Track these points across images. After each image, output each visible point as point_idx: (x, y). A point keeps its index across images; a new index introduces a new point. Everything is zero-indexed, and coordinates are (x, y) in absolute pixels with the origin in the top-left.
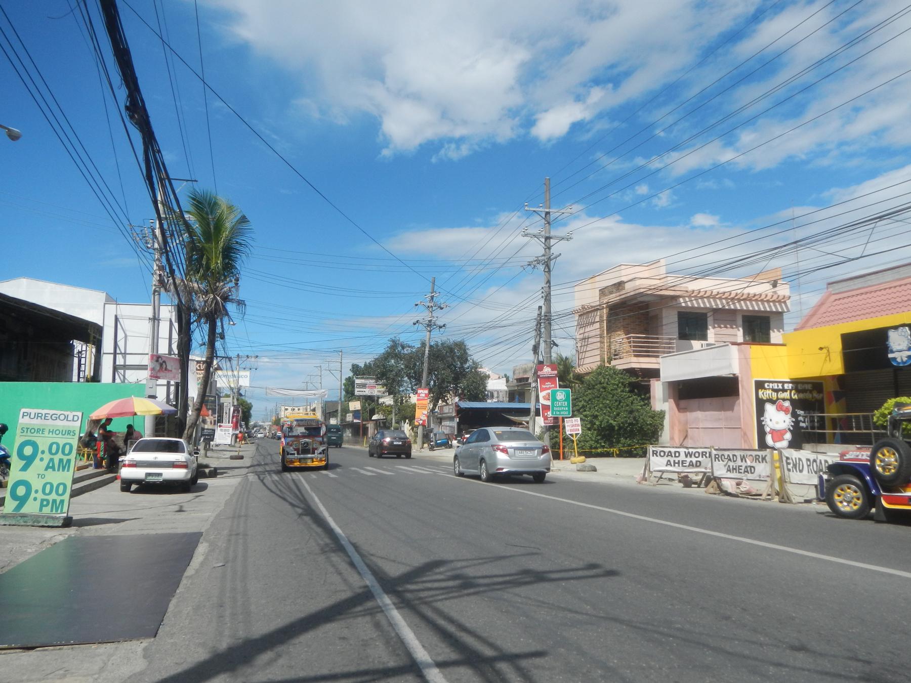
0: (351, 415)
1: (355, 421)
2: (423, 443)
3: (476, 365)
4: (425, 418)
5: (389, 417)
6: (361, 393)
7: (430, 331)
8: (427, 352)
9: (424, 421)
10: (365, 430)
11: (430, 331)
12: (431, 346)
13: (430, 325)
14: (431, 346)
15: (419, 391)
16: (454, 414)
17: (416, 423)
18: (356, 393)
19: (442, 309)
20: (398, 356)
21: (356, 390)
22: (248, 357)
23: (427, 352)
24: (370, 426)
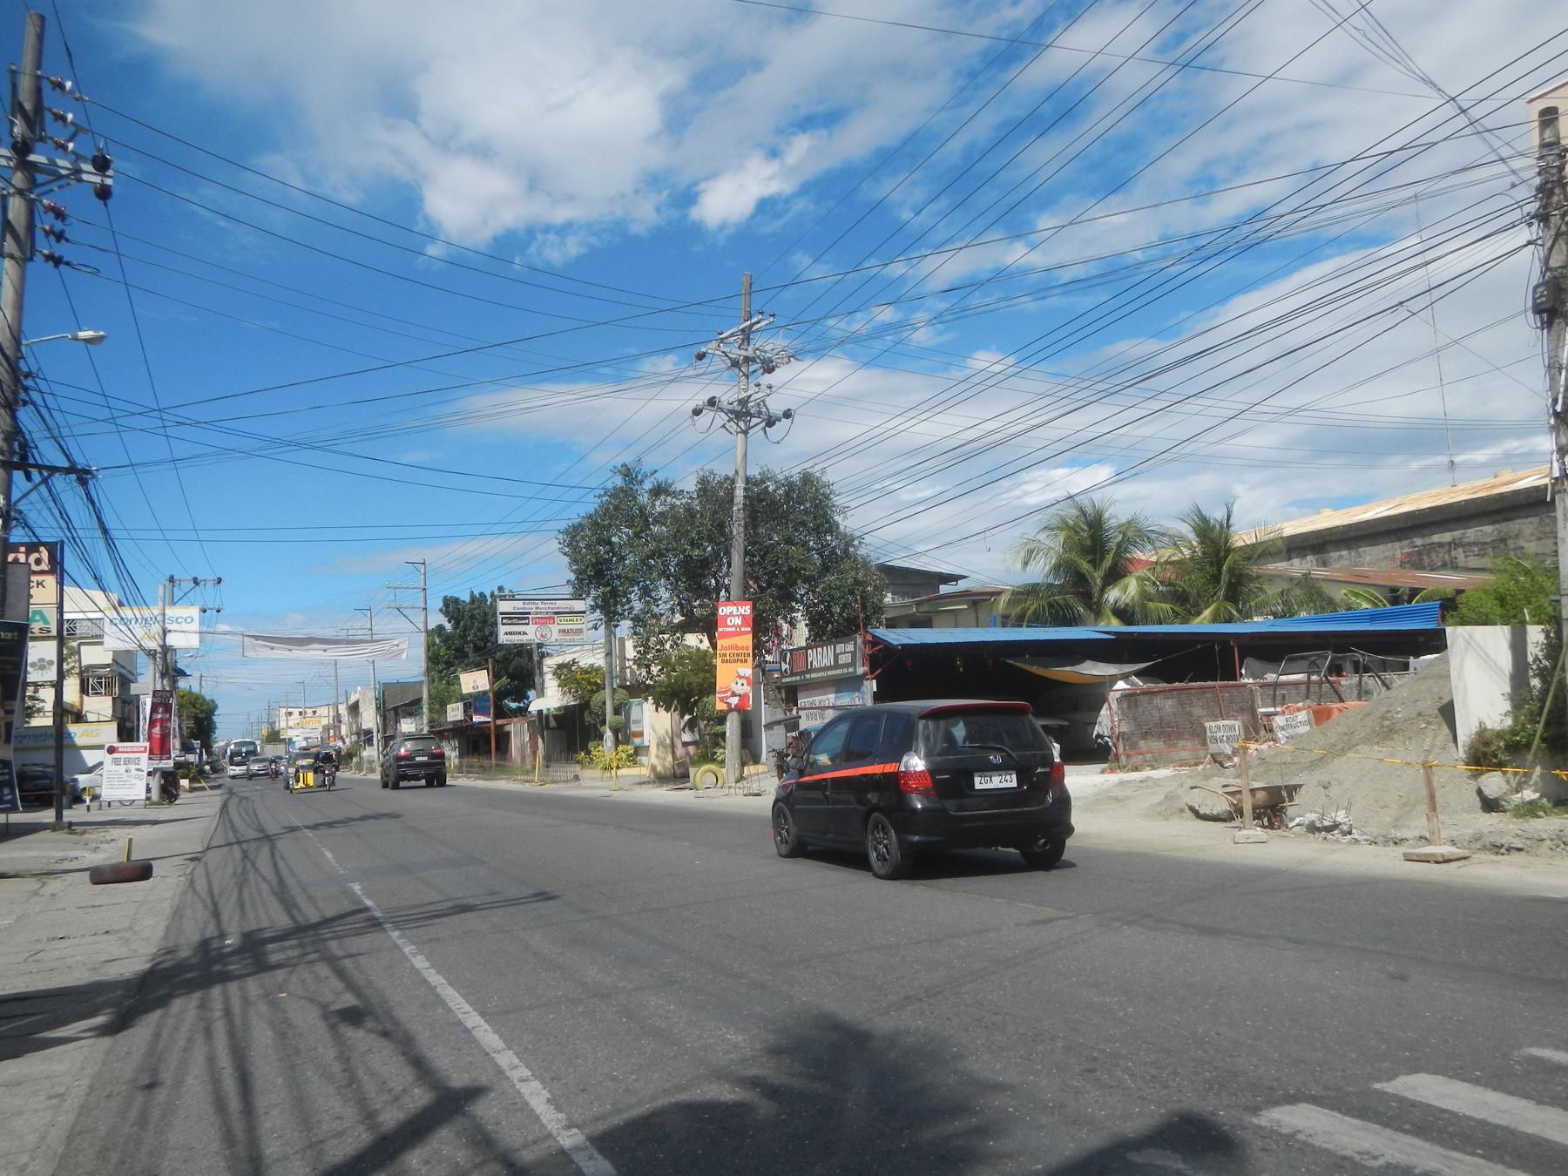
0: (460, 705)
1: (476, 719)
2: (743, 764)
3: (848, 541)
4: (747, 689)
5: (597, 698)
6: (516, 639)
7: (745, 433)
8: (739, 493)
9: (743, 697)
10: (503, 738)
11: (745, 433)
12: (748, 480)
13: (741, 413)
14: (748, 480)
15: (724, 610)
16: (861, 670)
17: (720, 706)
18: (503, 639)
19: (770, 370)
20: (640, 521)
21: (502, 629)
22: (196, 581)
23: (739, 493)
24: (518, 732)
